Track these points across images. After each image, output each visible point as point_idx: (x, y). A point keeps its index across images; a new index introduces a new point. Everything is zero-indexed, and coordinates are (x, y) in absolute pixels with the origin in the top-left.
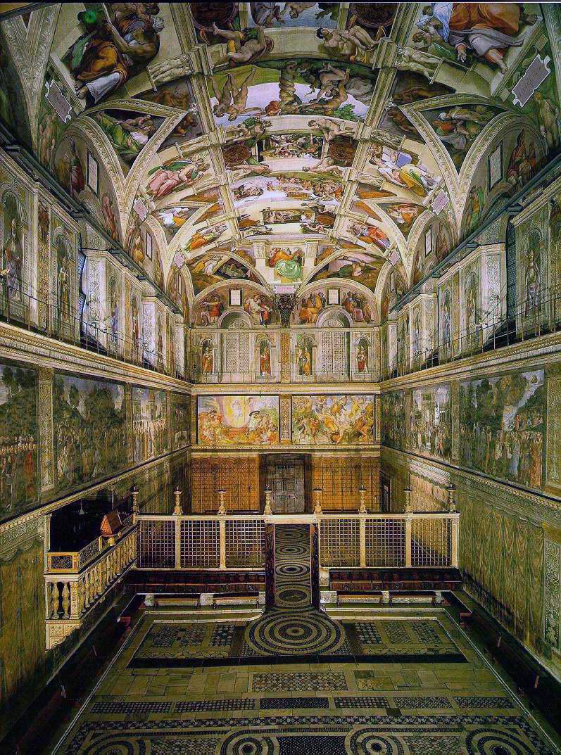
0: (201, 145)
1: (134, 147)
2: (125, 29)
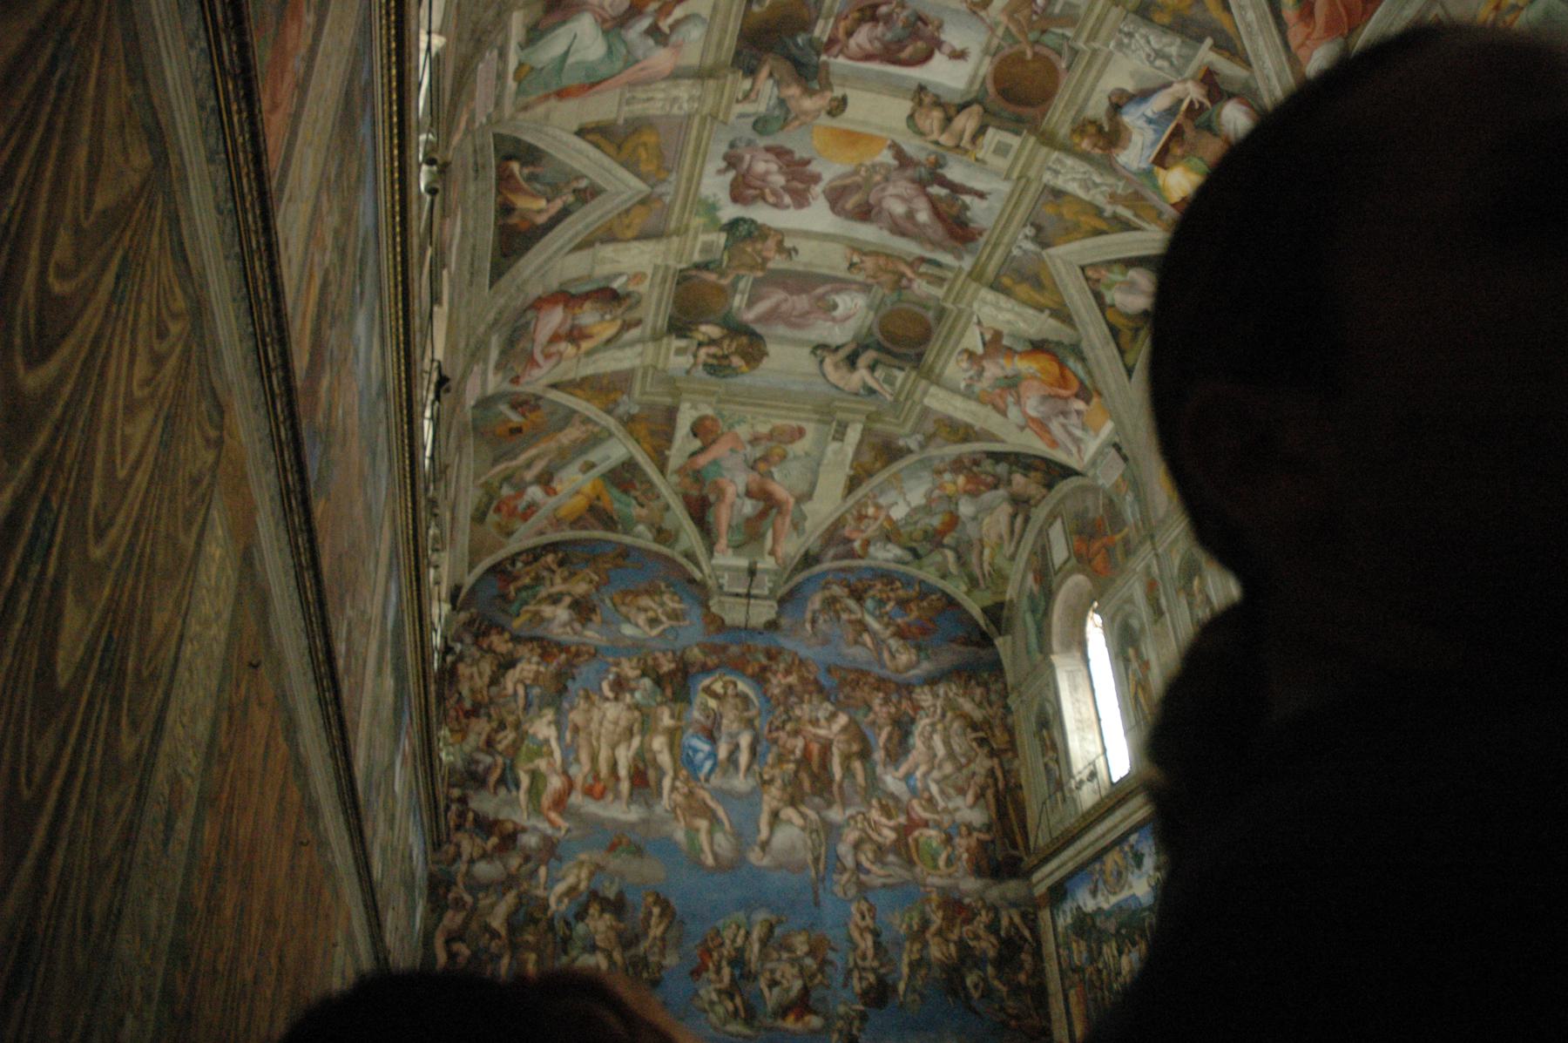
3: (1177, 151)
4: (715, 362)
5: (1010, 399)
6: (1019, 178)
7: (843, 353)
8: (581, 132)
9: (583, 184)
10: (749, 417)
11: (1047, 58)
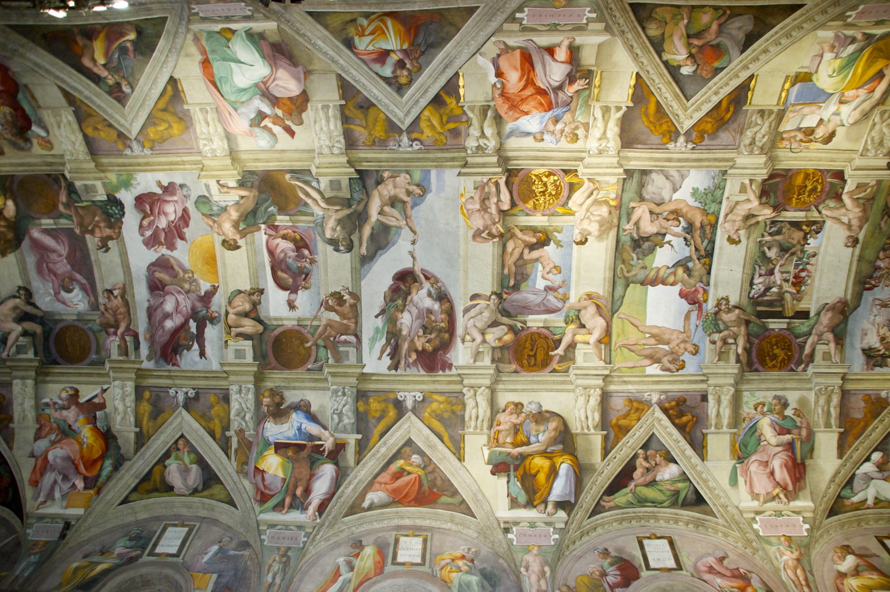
0: (726, 399)
1: (680, 485)
2: (525, 440)
3: (290, 453)
5: (53, 437)
6: (225, 372)
7: (29, 309)
8: (173, 81)
9: (126, 89)
11: (310, 356)
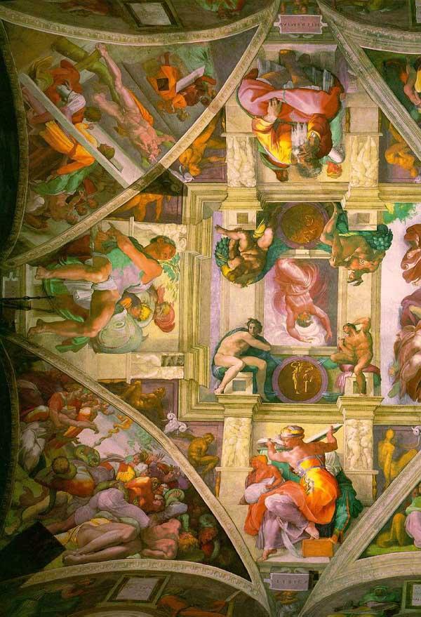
4: (231, 247)
5: (270, 481)
7: (255, 343)
10: (178, 282)
